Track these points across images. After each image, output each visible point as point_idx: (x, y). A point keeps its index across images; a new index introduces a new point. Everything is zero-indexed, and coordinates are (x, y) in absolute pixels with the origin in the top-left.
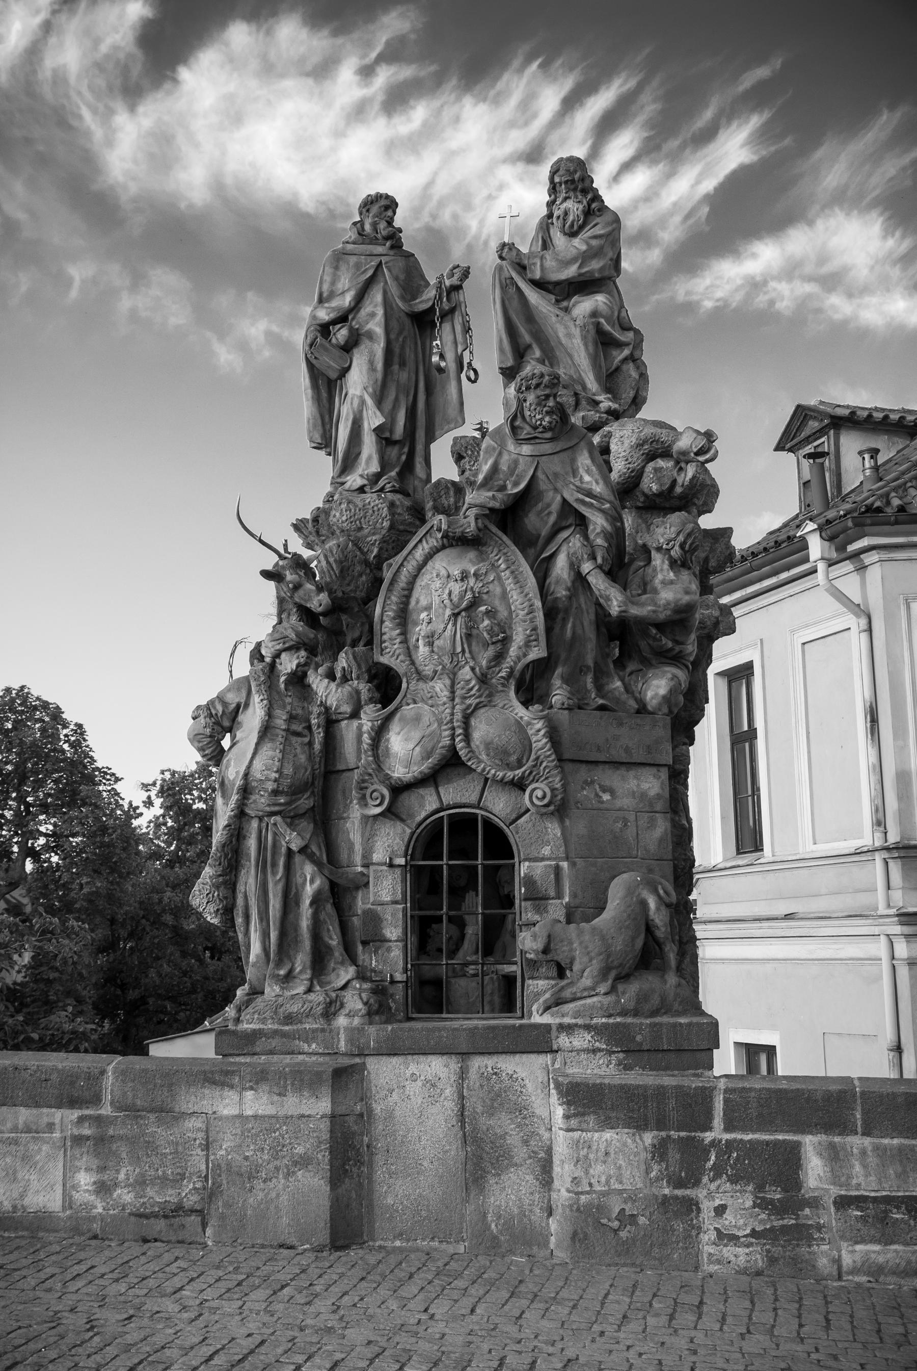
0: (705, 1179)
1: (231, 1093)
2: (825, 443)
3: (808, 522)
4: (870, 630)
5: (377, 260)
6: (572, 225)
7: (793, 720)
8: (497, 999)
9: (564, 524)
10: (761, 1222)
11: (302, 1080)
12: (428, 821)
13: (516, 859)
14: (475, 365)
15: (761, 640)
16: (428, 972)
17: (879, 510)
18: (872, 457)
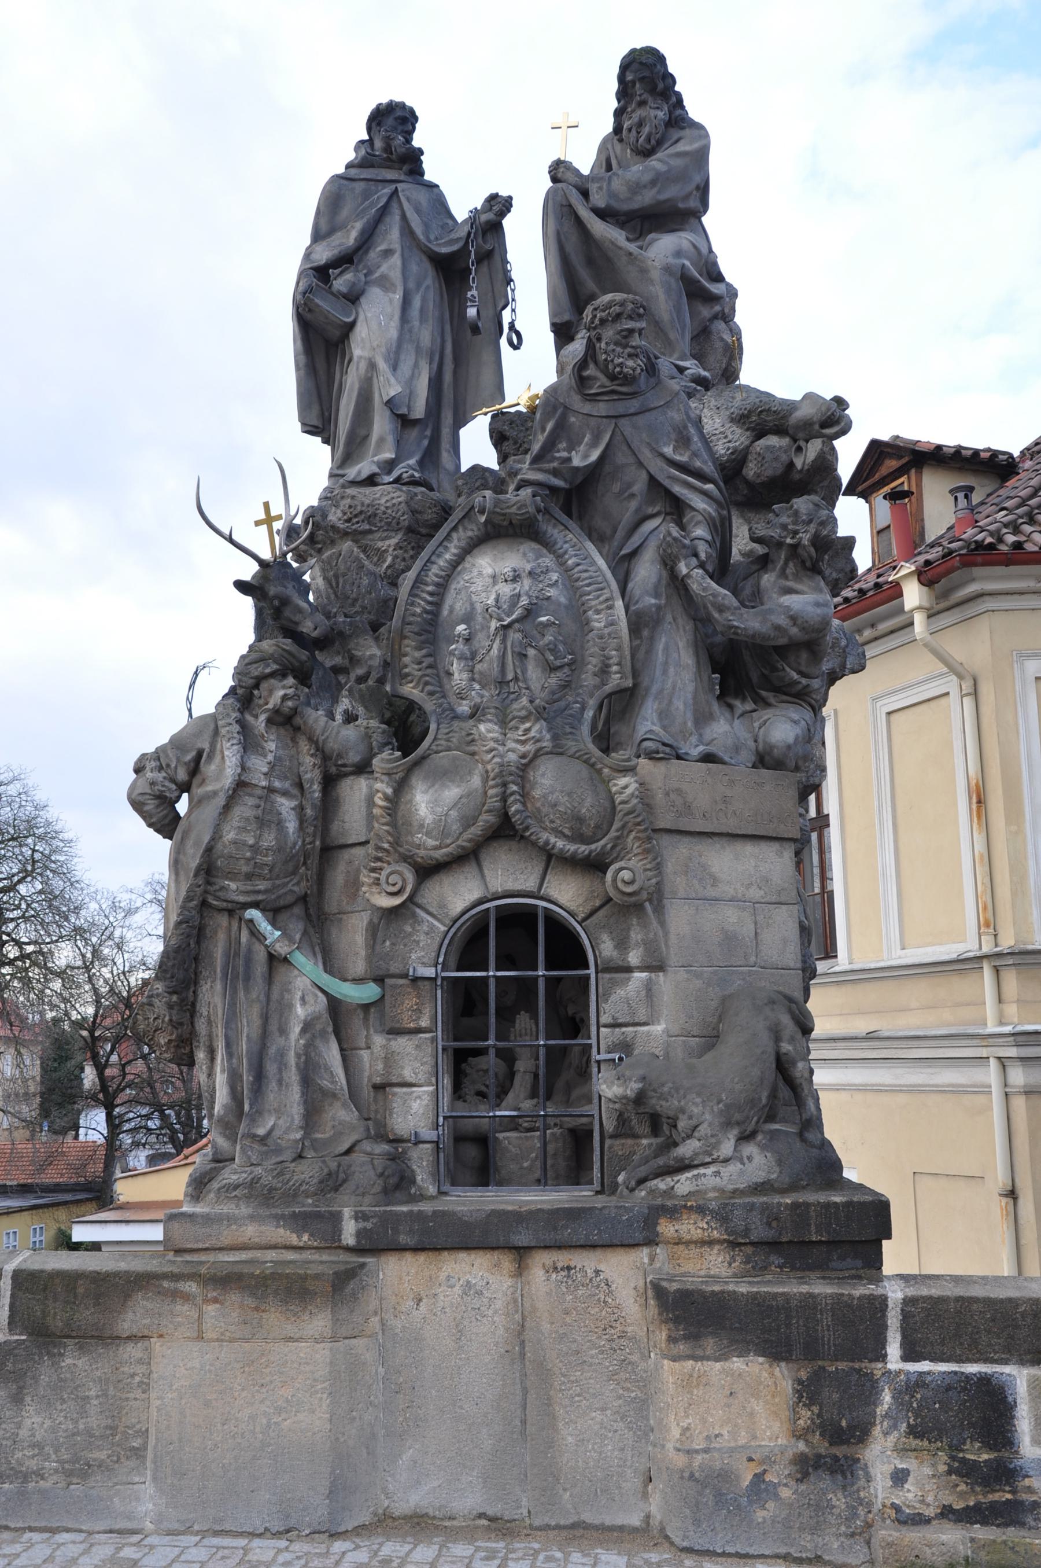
0: (877, 1431)
1: (186, 1308)
2: (902, 482)
3: (903, 563)
4: (975, 693)
5: (393, 187)
6: (648, 139)
7: (876, 803)
8: (562, 1163)
9: (651, 510)
10: (962, 1495)
13: (592, 971)
14: (518, 327)
16: (468, 1126)
17: (991, 547)
18: (966, 497)
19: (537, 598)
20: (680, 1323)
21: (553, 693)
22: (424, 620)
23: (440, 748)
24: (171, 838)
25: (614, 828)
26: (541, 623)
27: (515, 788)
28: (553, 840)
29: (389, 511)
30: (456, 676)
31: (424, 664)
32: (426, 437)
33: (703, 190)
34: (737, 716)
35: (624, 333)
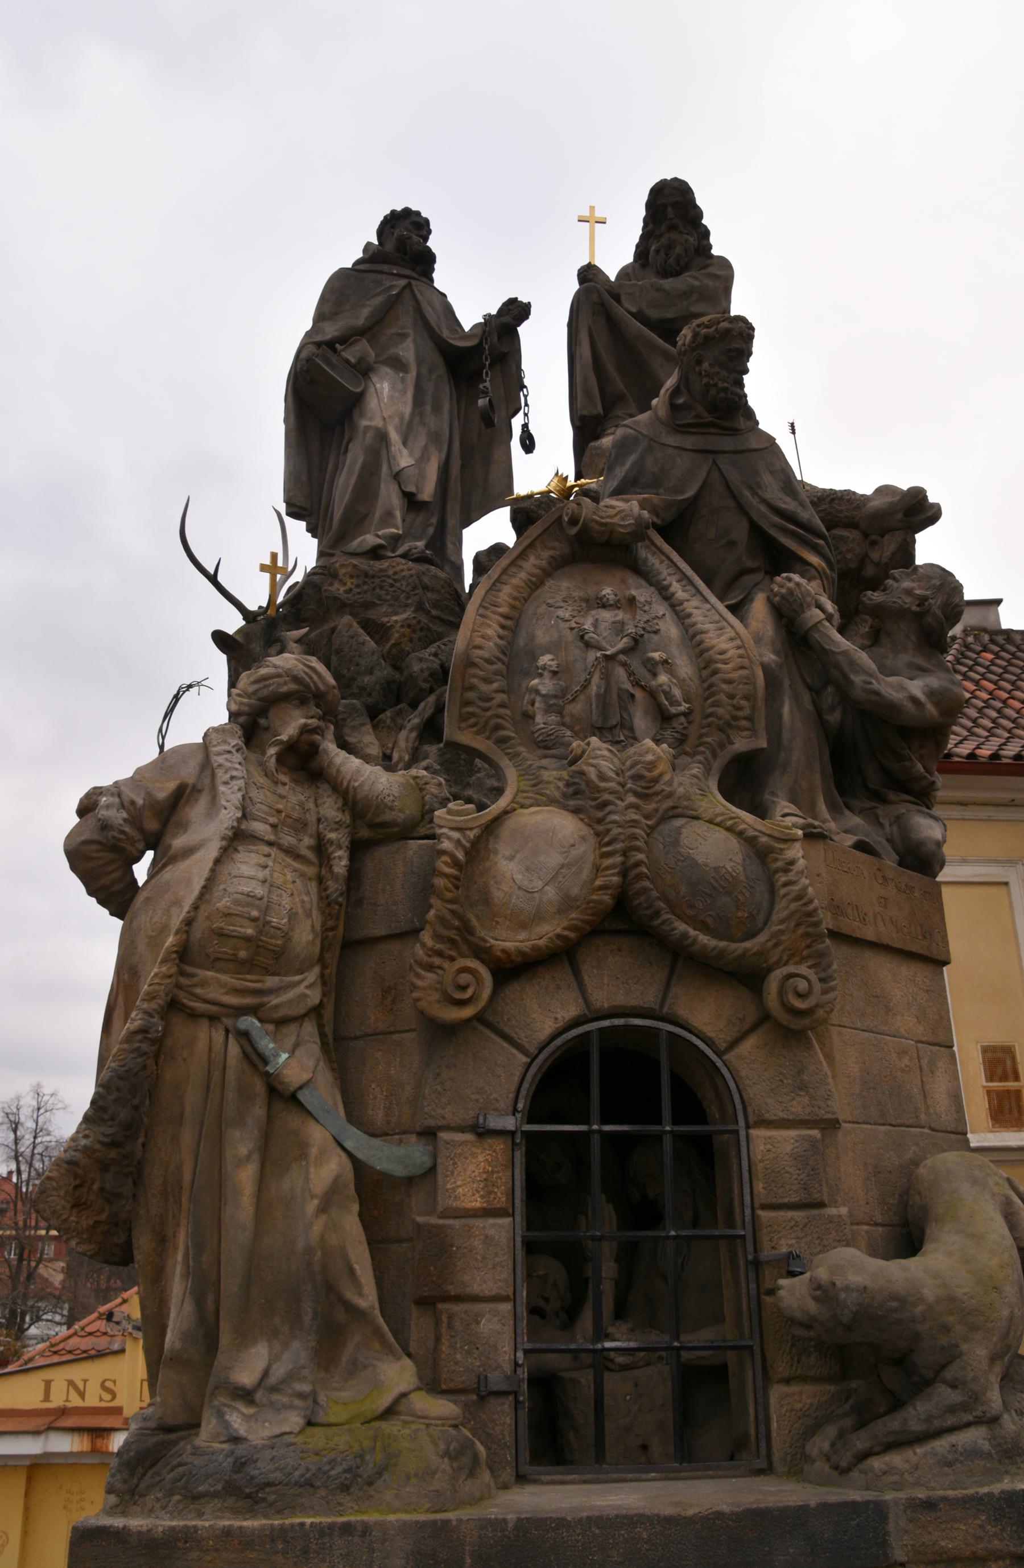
9: (750, 564)
12: (559, 1041)
14: (532, 429)
22: (497, 645)
23: (527, 802)
24: (121, 916)
25: (775, 917)
26: (652, 659)
27: (641, 856)
28: (692, 932)
29: (398, 584)
30: (539, 718)
31: (494, 702)
32: (431, 524)
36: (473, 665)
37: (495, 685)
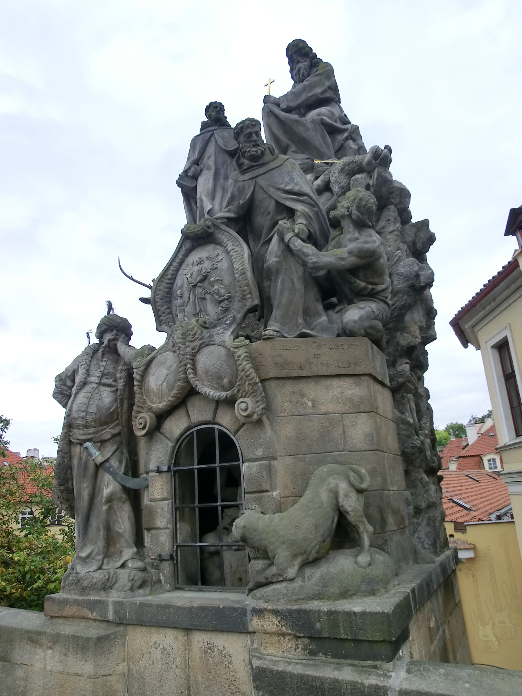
5: (212, 132)
11: (78, 644)
15: (509, 324)
19: (211, 269)
20: (259, 690)
21: (219, 315)
22: (164, 292)
26: (211, 281)
27: (189, 366)
31: (166, 313)
33: (334, 88)
34: (335, 312)
35: (248, 136)
36: (157, 302)
37: (165, 307)
